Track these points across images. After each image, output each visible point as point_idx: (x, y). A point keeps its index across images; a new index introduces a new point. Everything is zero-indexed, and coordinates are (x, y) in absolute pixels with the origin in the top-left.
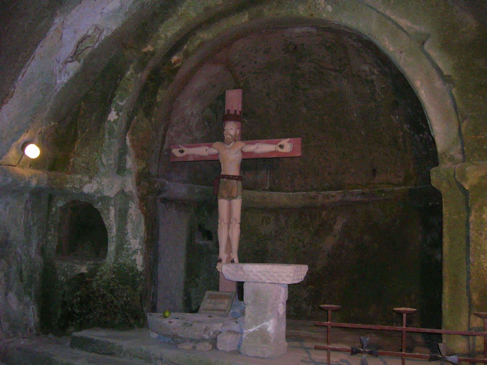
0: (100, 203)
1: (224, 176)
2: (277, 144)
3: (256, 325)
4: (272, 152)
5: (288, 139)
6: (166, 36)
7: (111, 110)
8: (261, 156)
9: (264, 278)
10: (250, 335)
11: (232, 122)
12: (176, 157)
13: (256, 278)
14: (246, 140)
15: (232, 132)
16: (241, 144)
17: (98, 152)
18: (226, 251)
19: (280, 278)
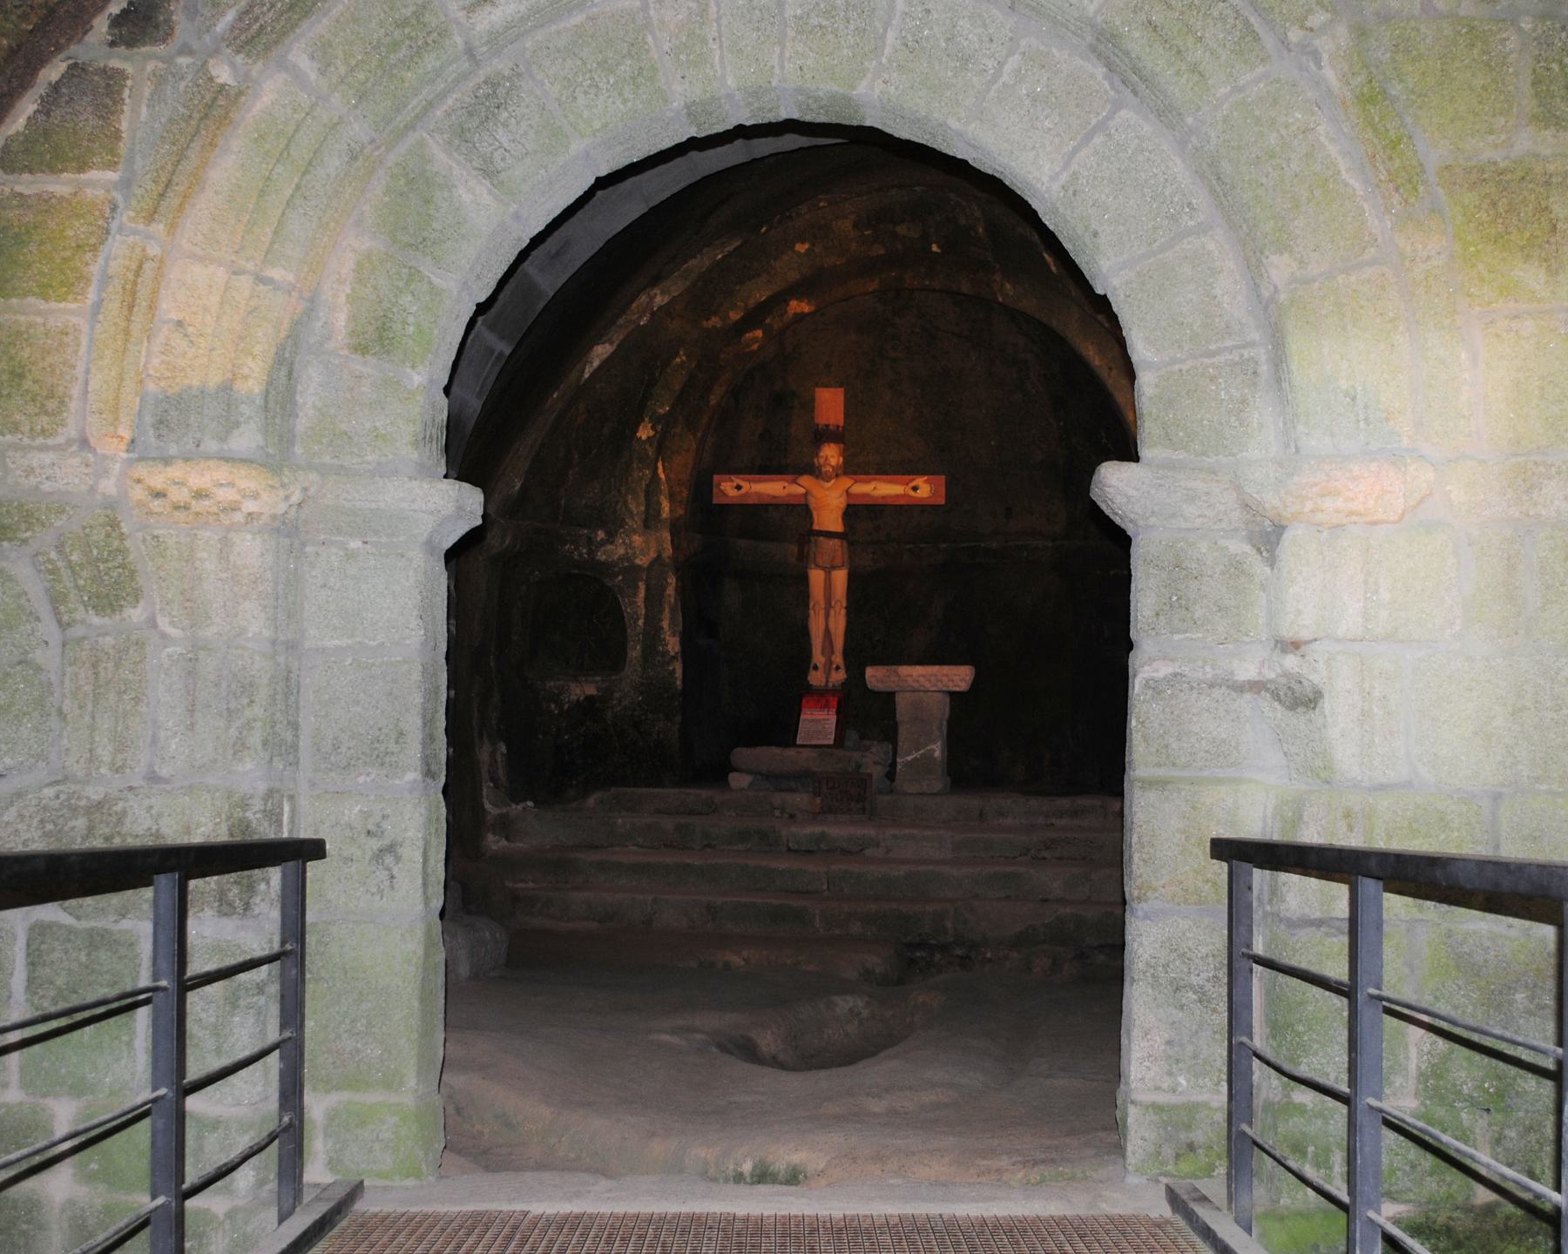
0: (620, 578)
2: (907, 484)
3: (918, 750)
4: (898, 496)
5: (926, 478)
7: (643, 420)
9: (928, 685)
10: (909, 765)
11: (832, 445)
12: (725, 495)
13: (916, 685)
14: (855, 473)
15: (833, 462)
16: (846, 482)
17: (619, 491)
18: (823, 653)
19: (951, 684)
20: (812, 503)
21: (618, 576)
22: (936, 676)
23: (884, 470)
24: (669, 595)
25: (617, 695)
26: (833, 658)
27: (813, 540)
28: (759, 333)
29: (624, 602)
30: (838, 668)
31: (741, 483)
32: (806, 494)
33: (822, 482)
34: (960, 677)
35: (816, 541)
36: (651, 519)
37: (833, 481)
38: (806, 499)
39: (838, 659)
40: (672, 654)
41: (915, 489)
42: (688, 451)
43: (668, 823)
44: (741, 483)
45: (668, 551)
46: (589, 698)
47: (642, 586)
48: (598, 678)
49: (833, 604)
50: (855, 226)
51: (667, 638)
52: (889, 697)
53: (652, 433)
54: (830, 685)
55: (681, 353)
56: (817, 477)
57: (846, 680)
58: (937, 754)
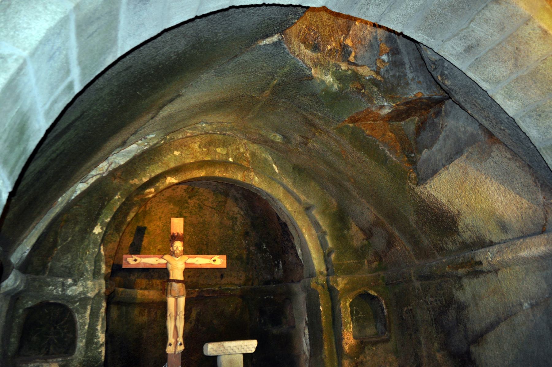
0: (78, 304)
1: (174, 281)
4: (207, 264)
5: (219, 256)
6: (151, 175)
7: (97, 225)
8: (199, 267)
12: (128, 263)
13: (231, 351)
16: (185, 257)
17: (82, 259)
18: (173, 337)
20: (170, 267)
21: (76, 302)
22: (241, 346)
23: (199, 252)
24: (102, 312)
26: (178, 339)
27: (170, 284)
28: (153, 190)
29: (77, 317)
30: (181, 344)
31: (137, 258)
32: (166, 264)
33: (174, 258)
34: (251, 346)
35: (171, 285)
36: (96, 274)
37: (179, 257)
38: (166, 266)
39: (181, 340)
40: (101, 343)
41: (214, 261)
42: (115, 241)
44: (137, 258)
45: (104, 290)
47: (89, 307)
48: (60, 360)
49: (178, 313)
50: (199, 147)
51: (100, 334)
52: (214, 359)
53: (100, 231)
54: (177, 353)
55: (119, 194)
56: (172, 255)
57: (184, 349)
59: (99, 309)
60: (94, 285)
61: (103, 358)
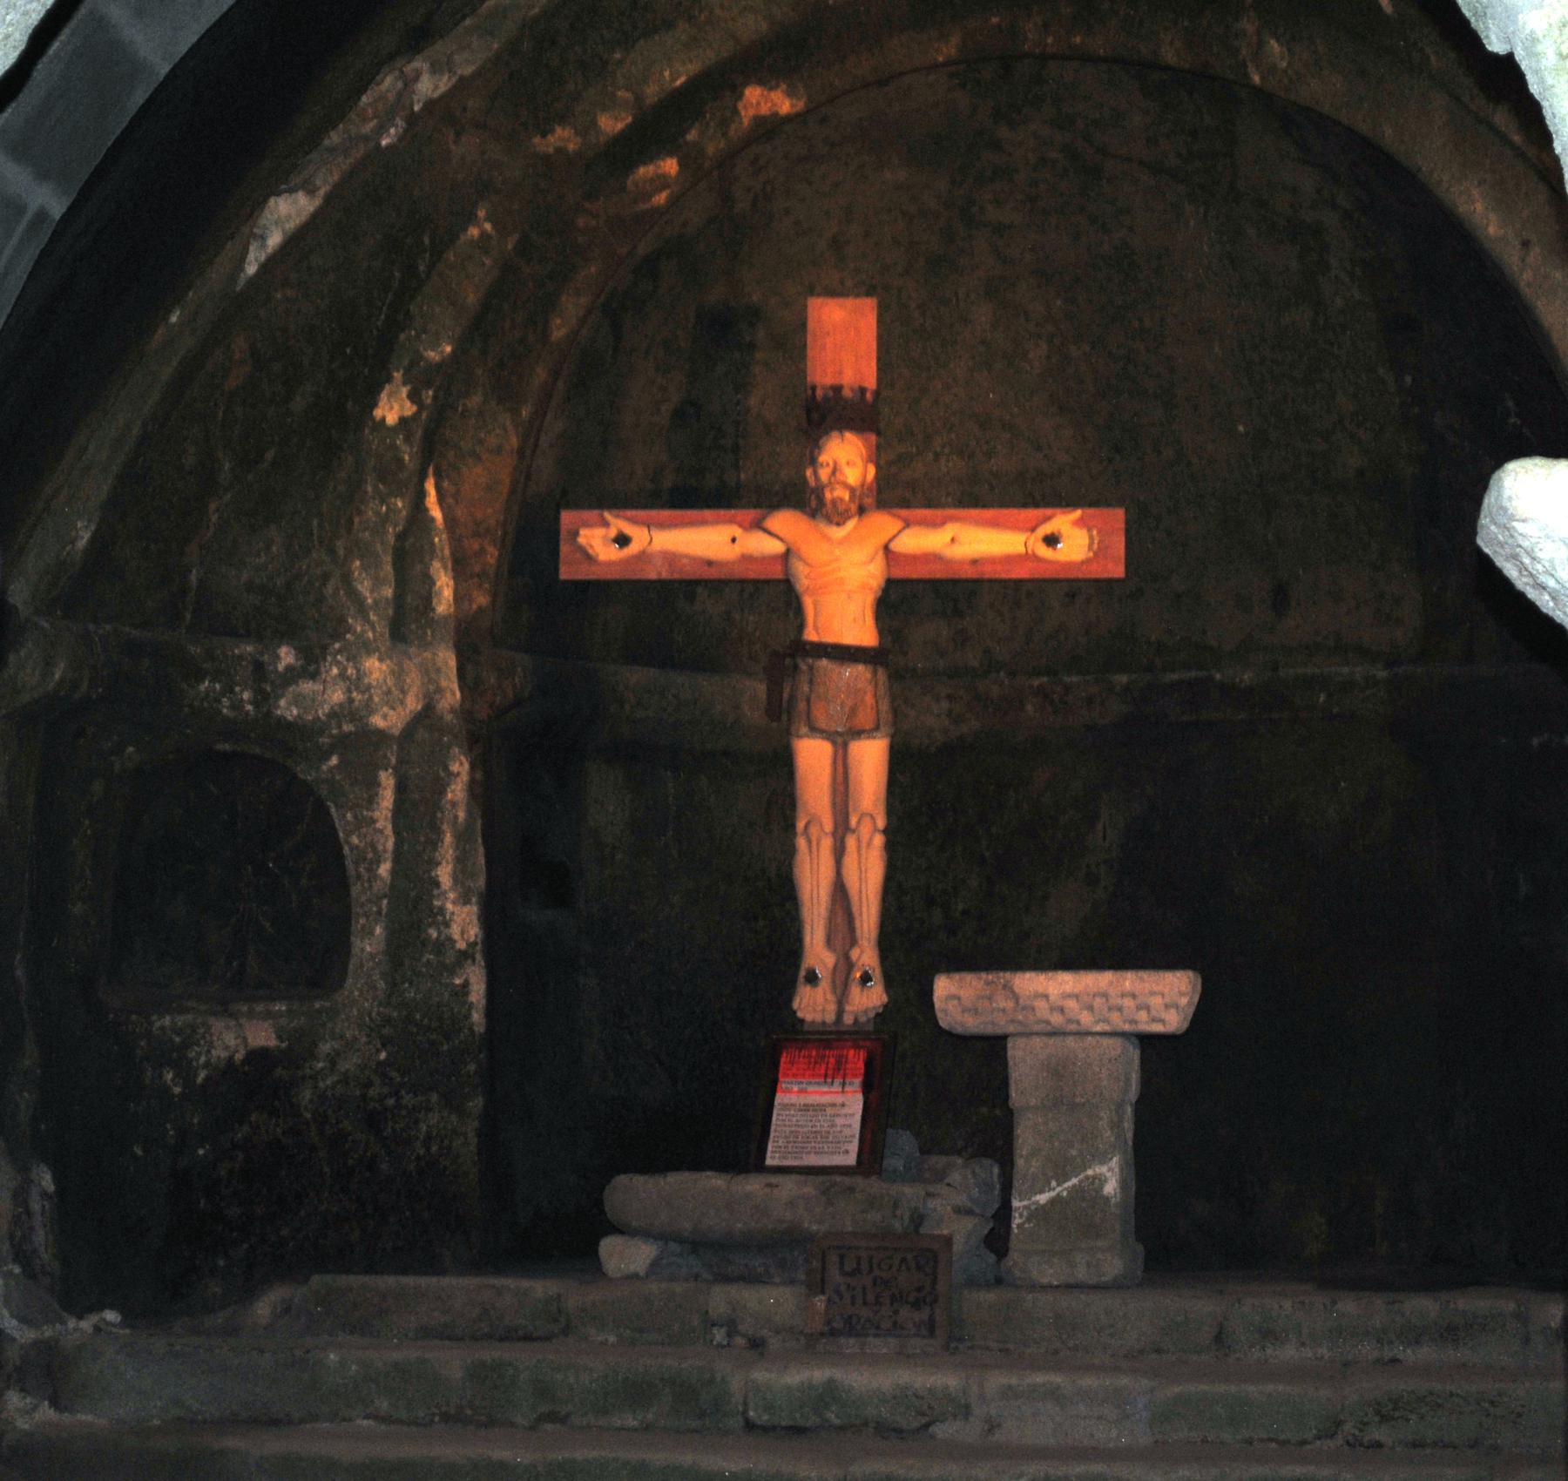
0: (334, 761)
2: (1033, 530)
3: (1062, 1177)
4: (1009, 559)
5: (1078, 513)
6: (639, 98)
7: (389, 379)
8: (969, 573)
9: (1086, 1019)
10: (1039, 1214)
11: (848, 435)
12: (589, 558)
13: (1057, 1020)
14: (906, 504)
15: (852, 476)
16: (883, 525)
17: (332, 551)
18: (829, 942)
19: (1143, 1015)
20: (802, 576)
21: (328, 758)
22: (1105, 995)
24: (454, 804)
25: (325, 1047)
26: (854, 954)
27: (804, 667)
28: (670, 166)
29: (342, 819)
30: (866, 978)
31: (629, 529)
32: (786, 556)
33: (823, 526)
35: (811, 668)
37: (851, 524)
39: (867, 956)
40: (461, 945)
41: (1051, 540)
42: (498, 450)
43: (452, 1362)
44: (629, 529)
45: (452, 695)
46: (259, 1057)
47: (387, 780)
49: (853, 821)
51: (449, 906)
52: (992, 1048)
53: (409, 409)
54: (848, 1020)
55: (481, 213)
56: (813, 514)
57: (886, 1006)
58: (1111, 1188)
59: (440, 787)
60: (399, 674)
61: (477, 1017)
